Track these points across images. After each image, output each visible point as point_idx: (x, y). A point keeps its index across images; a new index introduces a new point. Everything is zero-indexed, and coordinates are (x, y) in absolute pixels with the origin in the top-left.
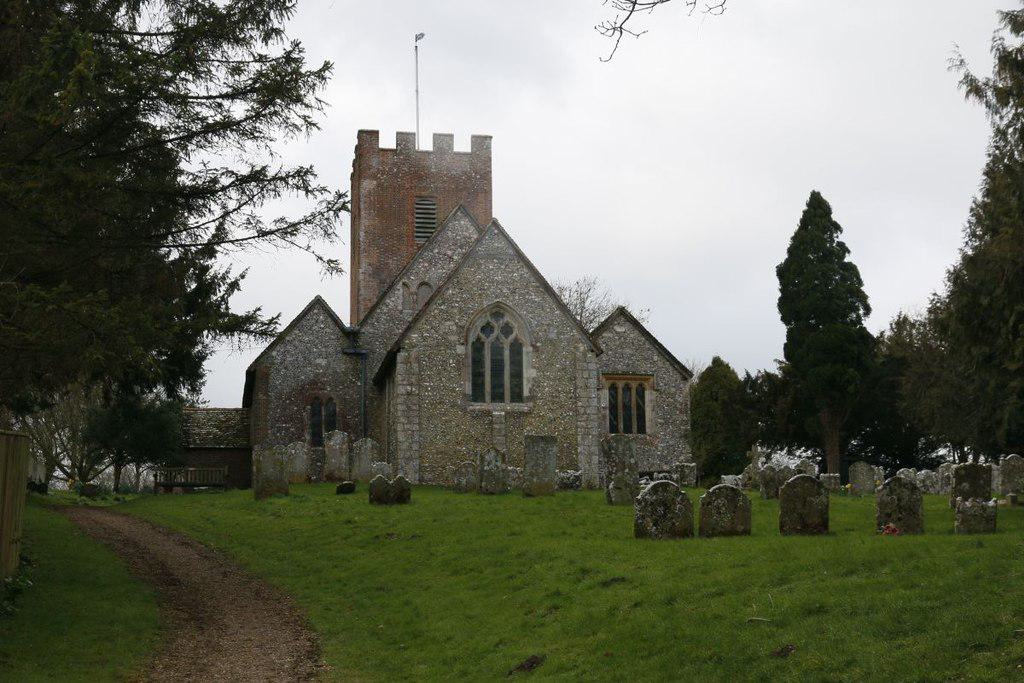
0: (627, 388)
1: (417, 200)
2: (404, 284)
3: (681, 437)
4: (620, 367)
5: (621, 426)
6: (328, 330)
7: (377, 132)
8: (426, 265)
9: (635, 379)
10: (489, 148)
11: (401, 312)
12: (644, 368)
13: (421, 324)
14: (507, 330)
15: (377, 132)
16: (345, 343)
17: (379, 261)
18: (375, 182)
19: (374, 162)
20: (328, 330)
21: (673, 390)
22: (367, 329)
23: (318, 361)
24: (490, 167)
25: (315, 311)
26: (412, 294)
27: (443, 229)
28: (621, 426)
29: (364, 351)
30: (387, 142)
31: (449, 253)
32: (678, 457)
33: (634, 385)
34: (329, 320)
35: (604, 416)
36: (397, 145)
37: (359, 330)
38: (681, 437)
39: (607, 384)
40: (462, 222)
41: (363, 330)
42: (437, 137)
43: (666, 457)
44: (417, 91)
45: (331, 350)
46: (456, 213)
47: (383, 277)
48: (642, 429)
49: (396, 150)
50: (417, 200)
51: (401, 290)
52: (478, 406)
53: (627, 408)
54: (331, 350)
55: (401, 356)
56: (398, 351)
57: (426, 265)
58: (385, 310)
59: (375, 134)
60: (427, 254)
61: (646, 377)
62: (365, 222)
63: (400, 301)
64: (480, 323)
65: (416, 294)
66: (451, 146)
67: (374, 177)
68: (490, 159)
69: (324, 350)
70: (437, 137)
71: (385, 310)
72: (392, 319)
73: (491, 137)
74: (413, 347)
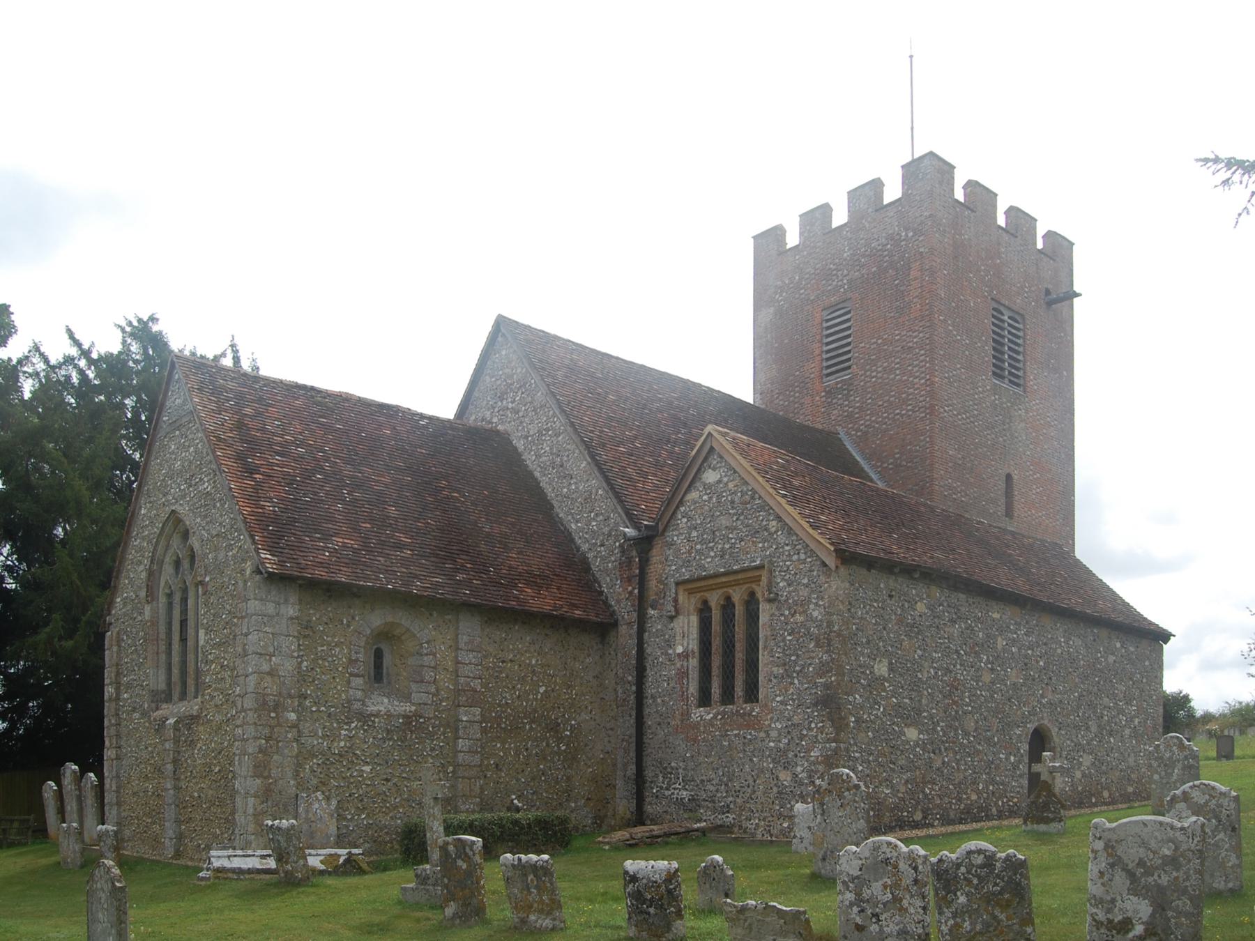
0: (728, 605)
3: (816, 704)
4: (712, 564)
5: (716, 690)
9: (737, 583)
21: (804, 593)
28: (716, 690)
32: (809, 751)
33: (738, 596)
35: (683, 674)
38: (816, 704)
39: (689, 603)
43: (785, 752)
48: (752, 694)
61: (751, 575)
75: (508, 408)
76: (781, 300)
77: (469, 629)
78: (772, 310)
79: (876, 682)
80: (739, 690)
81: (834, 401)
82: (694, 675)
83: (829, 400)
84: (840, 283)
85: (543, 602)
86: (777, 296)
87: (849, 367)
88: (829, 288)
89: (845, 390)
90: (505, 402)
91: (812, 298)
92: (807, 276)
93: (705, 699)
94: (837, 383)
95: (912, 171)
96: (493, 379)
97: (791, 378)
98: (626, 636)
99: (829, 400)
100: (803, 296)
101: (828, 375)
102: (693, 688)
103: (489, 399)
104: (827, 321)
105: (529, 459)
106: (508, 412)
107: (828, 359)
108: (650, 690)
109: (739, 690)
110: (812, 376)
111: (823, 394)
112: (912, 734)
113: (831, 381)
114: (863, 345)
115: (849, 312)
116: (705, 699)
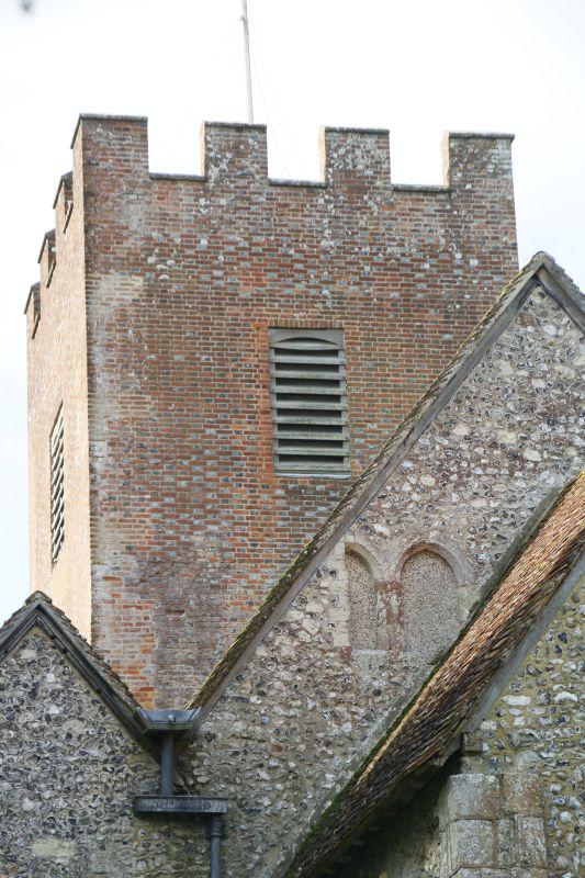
1: (278, 339)
2: (351, 553)
6: (77, 727)
7: (143, 122)
8: (429, 481)
10: (503, 172)
11: (346, 656)
13: (539, 651)
15: (143, 122)
16: (138, 773)
17: (161, 538)
18: (139, 282)
19: (135, 216)
20: (77, 727)
22: (224, 722)
23: (43, 848)
24: (514, 235)
25: (28, 654)
26: (382, 587)
27: (484, 351)
29: (215, 807)
31: (510, 438)
34: (80, 685)
36: (209, 162)
37: (196, 724)
40: (550, 330)
41: (206, 727)
42: (336, 137)
44: (245, 21)
45: (88, 804)
46: (526, 292)
47: (177, 588)
49: (204, 180)
50: (278, 339)
51: (343, 574)
54: (88, 804)
55: (465, 791)
56: (454, 764)
57: (429, 481)
58: (287, 648)
59: (133, 128)
60: (430, 444)
62: (104, 407)
63: (341, 615)
65: (398, 588)
66: (381, 167)
67: (135, 264)
68: (510, 207)
69: (61, 803)
70: (336, 137)
71: (287, 648)
72: (313, 682)
73: (511, 138)
74: (517, 749)
75: (571, 444)
76: (162, 271)
78: (139, 282)
81: (307, 514)
83: (297, 509)
84: (313, 292)
86: (151, 260)
87: (339, 459)
88: (288, 291)
89: (334, 499)
90: (560, 430)
91: (243, 295)
92: (232, 248)
94: (316, 481)
96: (524, 373)
97: (193, 436)
99: (297, 509)
100: (222, 283)
101: (284, 458)
103: (510, 406)
104: (279, 351)
106: (572, 452)
107: (282, 427)
110: (249, 448)
111: (280, 492)
114: (375, 426)
115: (334, 353)
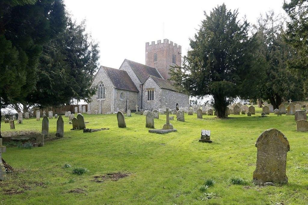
0: (151, 91)
4: (149, 87)
12: (153, 87)
14: (103, 85)
30: (150, 44)
33: (152, 90)
48: (153, 99)
52: (98, 100)
53: (151, 95)
61: (153, 89)
64: (99, 85)
77: (128, 93)
79: (164, 99)
80: (152, 99)
82: (147, 97)
85: (133, 90)
93: (148, 100)
95: (164, 40)
98: (140, 93)
102: (147, 99)
105: (129, 74)
108: (143, 98)
109: (152, 99)
112: (166, 103)
113: (155, 62)
116: (148, 100)
